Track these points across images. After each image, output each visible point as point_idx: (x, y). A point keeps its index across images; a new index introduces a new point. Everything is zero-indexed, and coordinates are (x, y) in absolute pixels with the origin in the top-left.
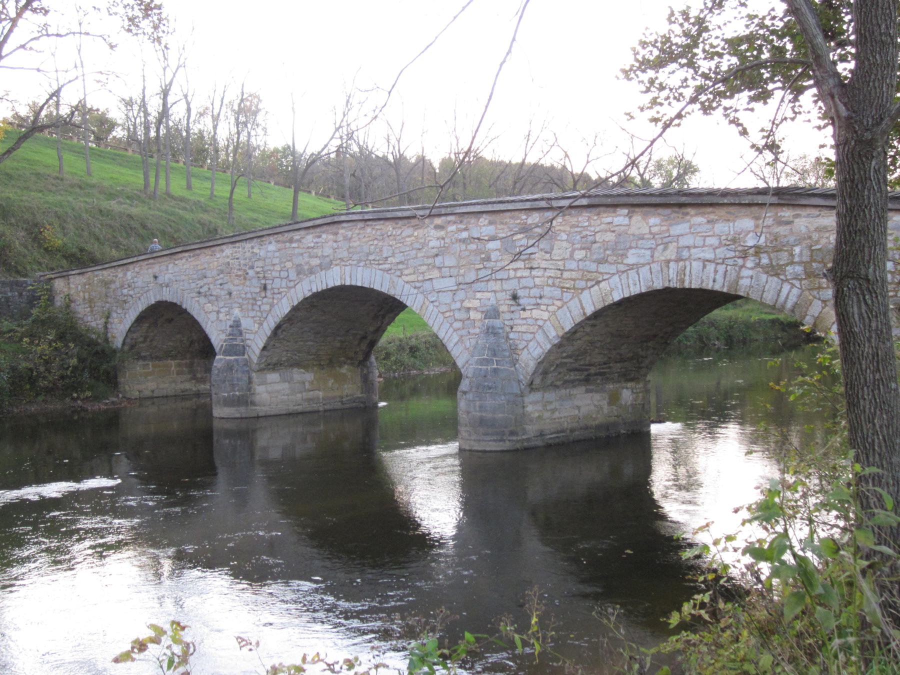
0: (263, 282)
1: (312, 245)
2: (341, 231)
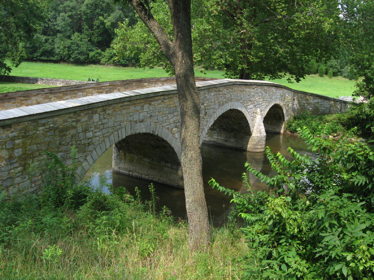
0: (206, 111)
1: (226, 93)
2: (234, 88)
